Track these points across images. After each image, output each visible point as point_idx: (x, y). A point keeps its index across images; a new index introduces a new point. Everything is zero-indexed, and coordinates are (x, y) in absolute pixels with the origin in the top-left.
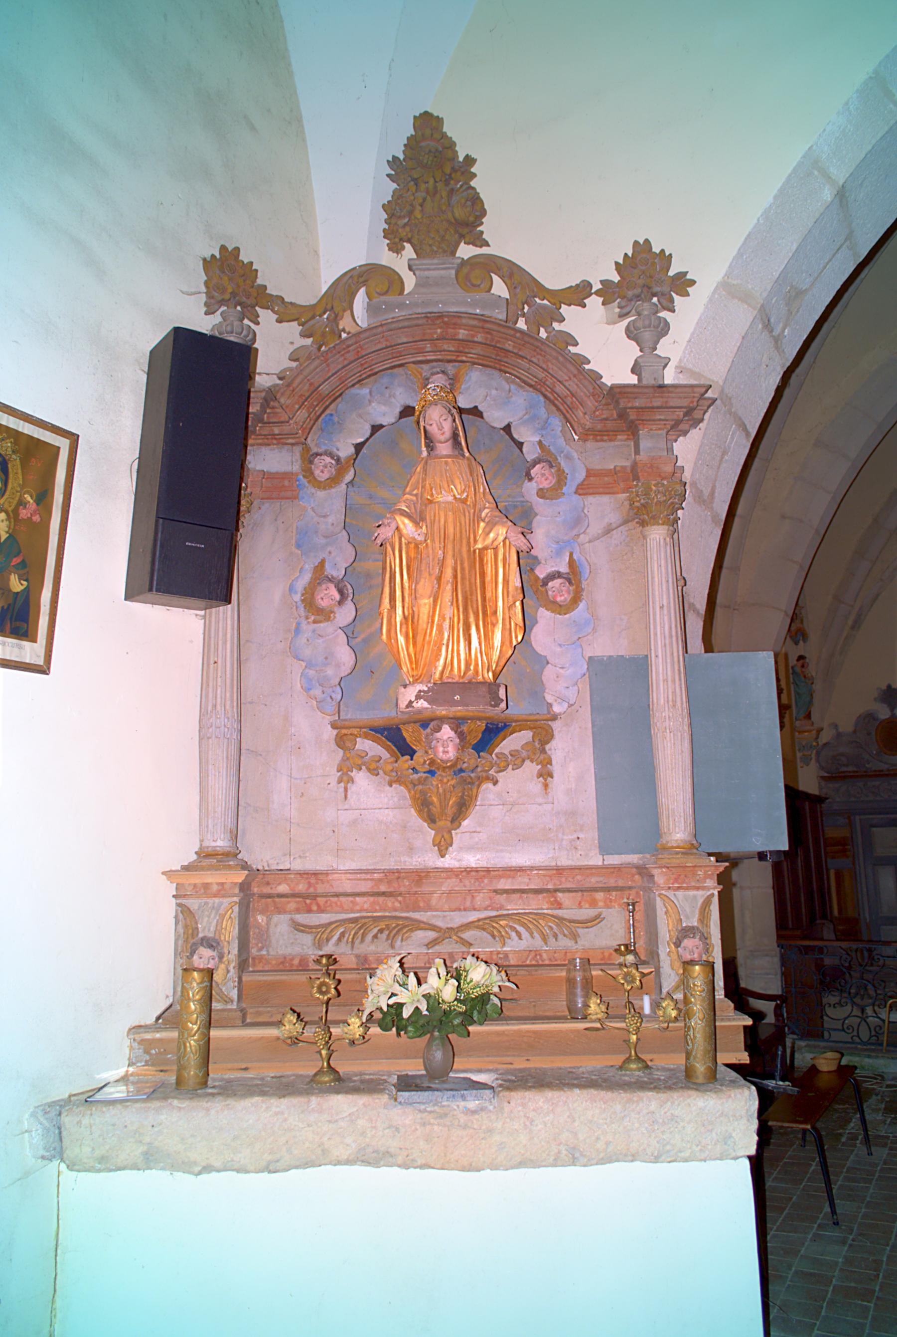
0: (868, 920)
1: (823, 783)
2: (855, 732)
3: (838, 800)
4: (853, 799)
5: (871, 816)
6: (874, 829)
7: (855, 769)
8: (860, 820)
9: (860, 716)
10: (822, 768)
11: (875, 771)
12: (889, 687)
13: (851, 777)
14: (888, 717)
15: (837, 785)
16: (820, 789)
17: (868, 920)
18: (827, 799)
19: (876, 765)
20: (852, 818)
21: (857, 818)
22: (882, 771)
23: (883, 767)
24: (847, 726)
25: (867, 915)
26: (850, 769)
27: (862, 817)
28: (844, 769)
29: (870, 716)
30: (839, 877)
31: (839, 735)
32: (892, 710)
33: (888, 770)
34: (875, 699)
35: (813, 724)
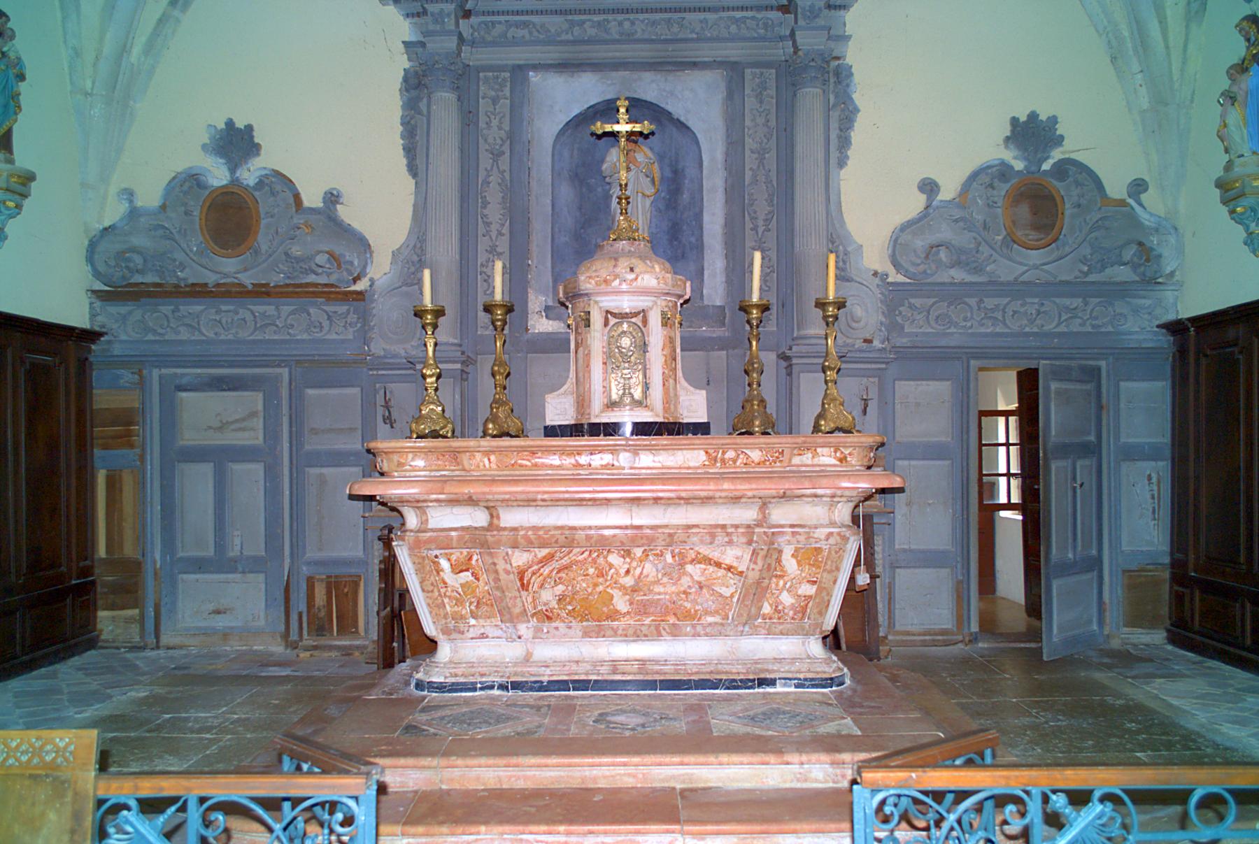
0: (158, 566)
1: (98, 304)
2: (163, 207)
3: (124, 337)
4: (150, 337)
5: (179, 371)
6: (184, 394)
7: (157, 280)
8: (161, 377)
9: (174, 178)
10: (97, 274)
11: (193, 285)
12: (230, 124)
13: (150, 295)
14: (225, 182)
15: (123, 309)
16: (93, 316)
17: (158, 566)
18: (100, 335)
19: (190, 275)
20: (145, 372)
21: (156, 373)
22: (206, 285)
23: (211, 279)
24: (150, 197)
25: (158, 557)
26: (150, 278)
27: (164, 371)
28: (138, 279)
29: (191, 181)
30: (113, 484)
31: (134, 213)
32: (233, 170)
33: (218, 285)
34: (204, 147)
35: (11, 162)
